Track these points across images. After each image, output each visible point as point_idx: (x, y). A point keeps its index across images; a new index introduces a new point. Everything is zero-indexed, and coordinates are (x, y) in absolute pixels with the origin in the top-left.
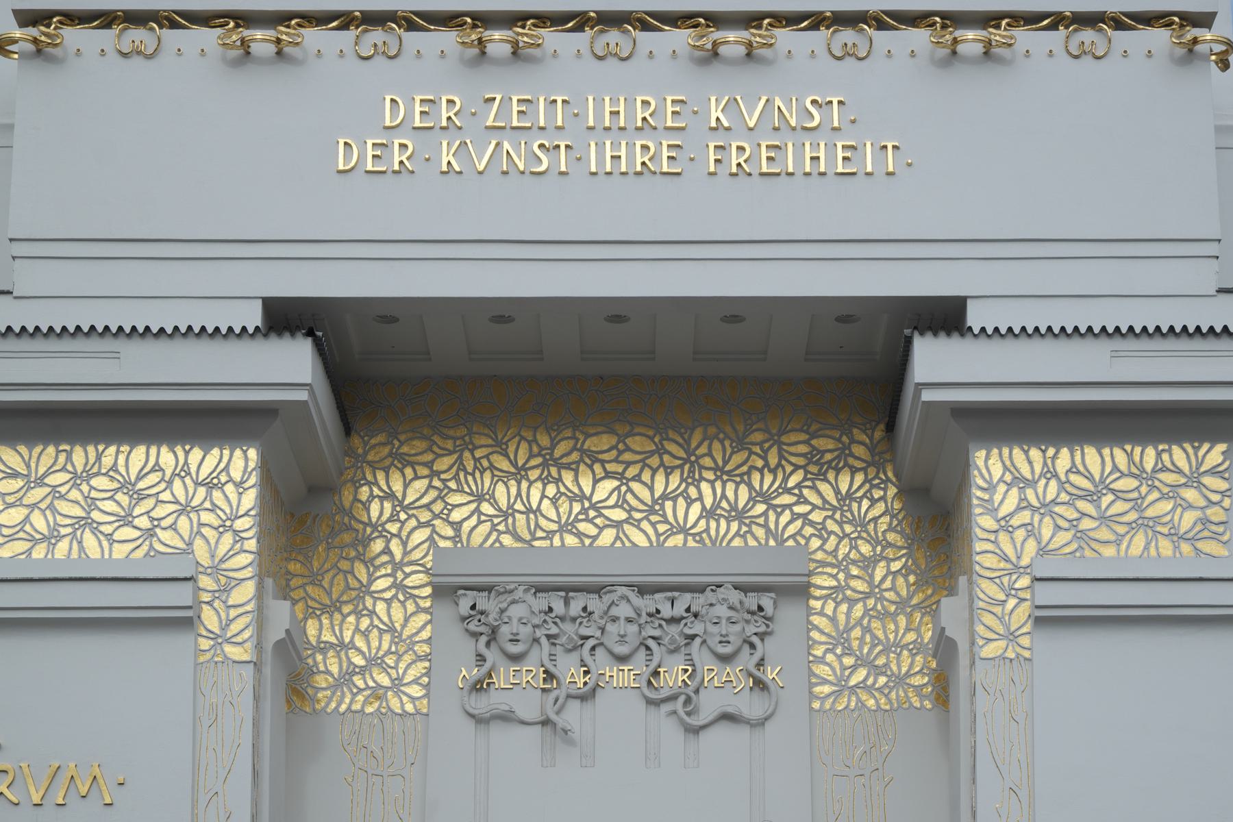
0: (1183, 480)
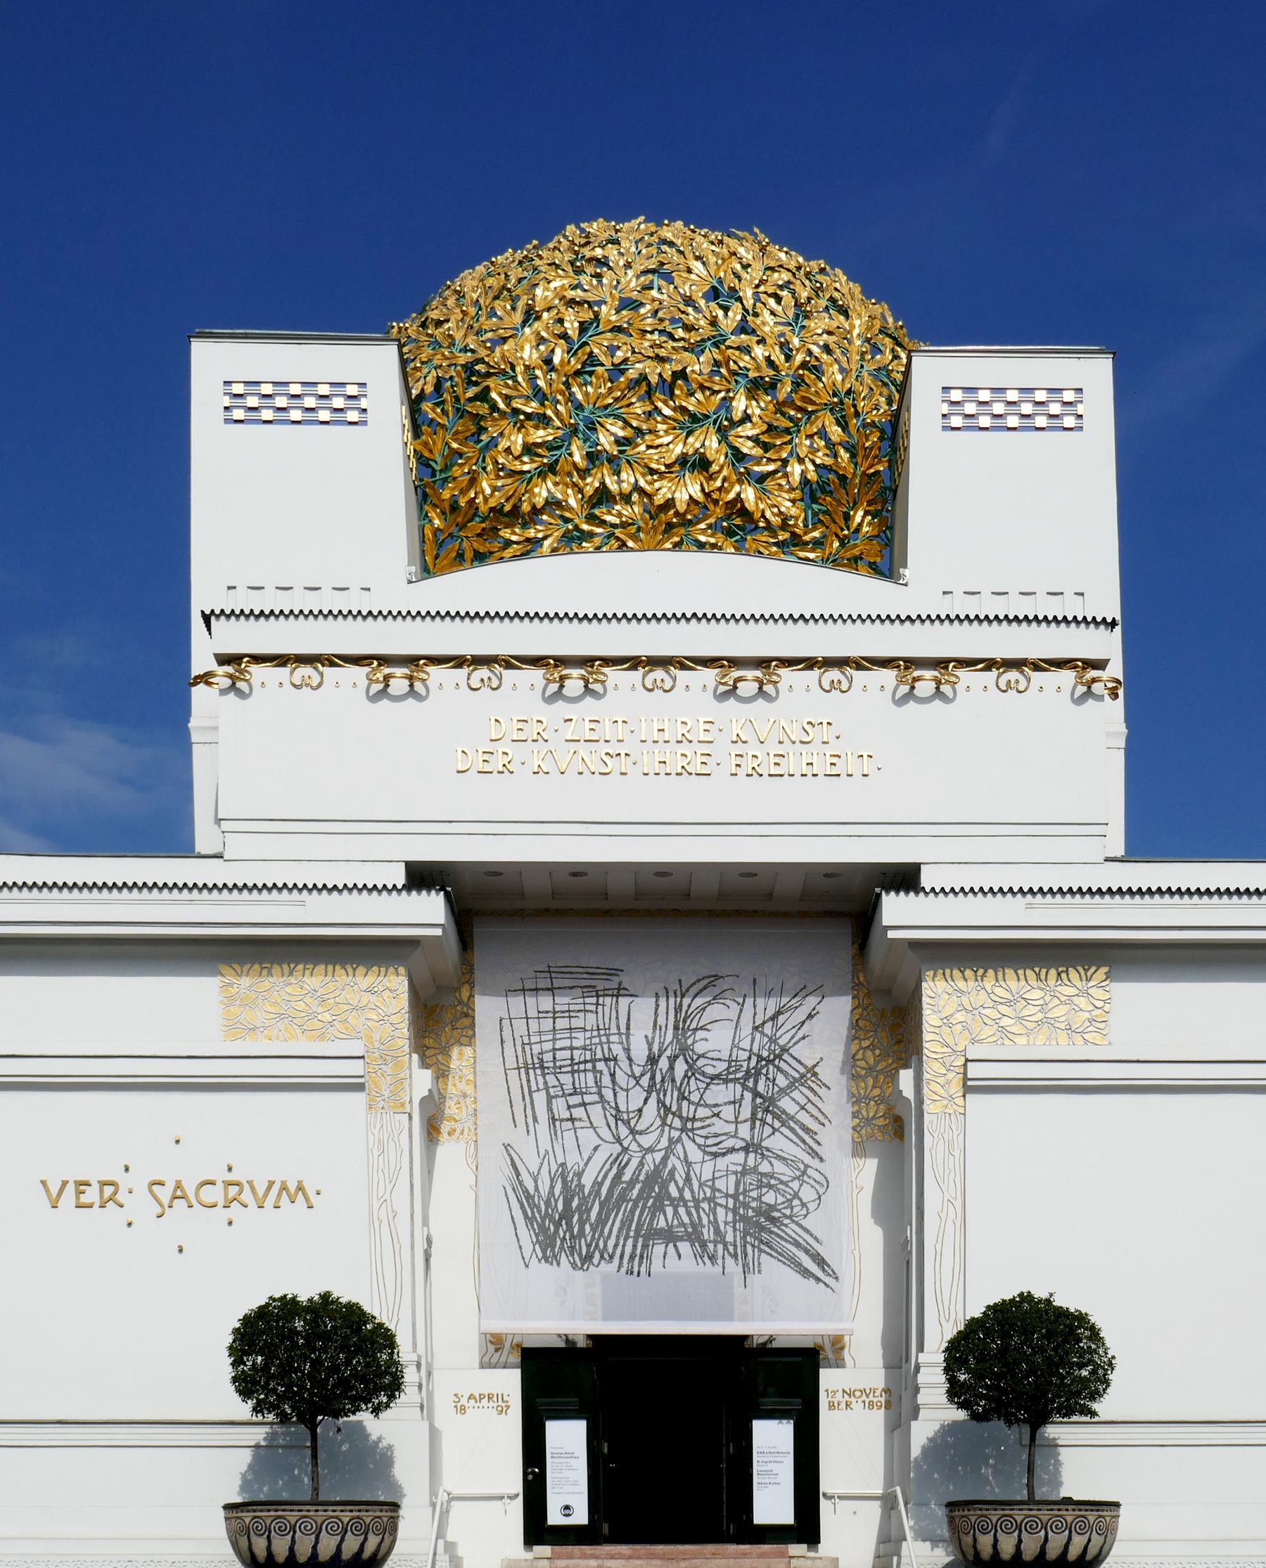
0: (1077, 992)
